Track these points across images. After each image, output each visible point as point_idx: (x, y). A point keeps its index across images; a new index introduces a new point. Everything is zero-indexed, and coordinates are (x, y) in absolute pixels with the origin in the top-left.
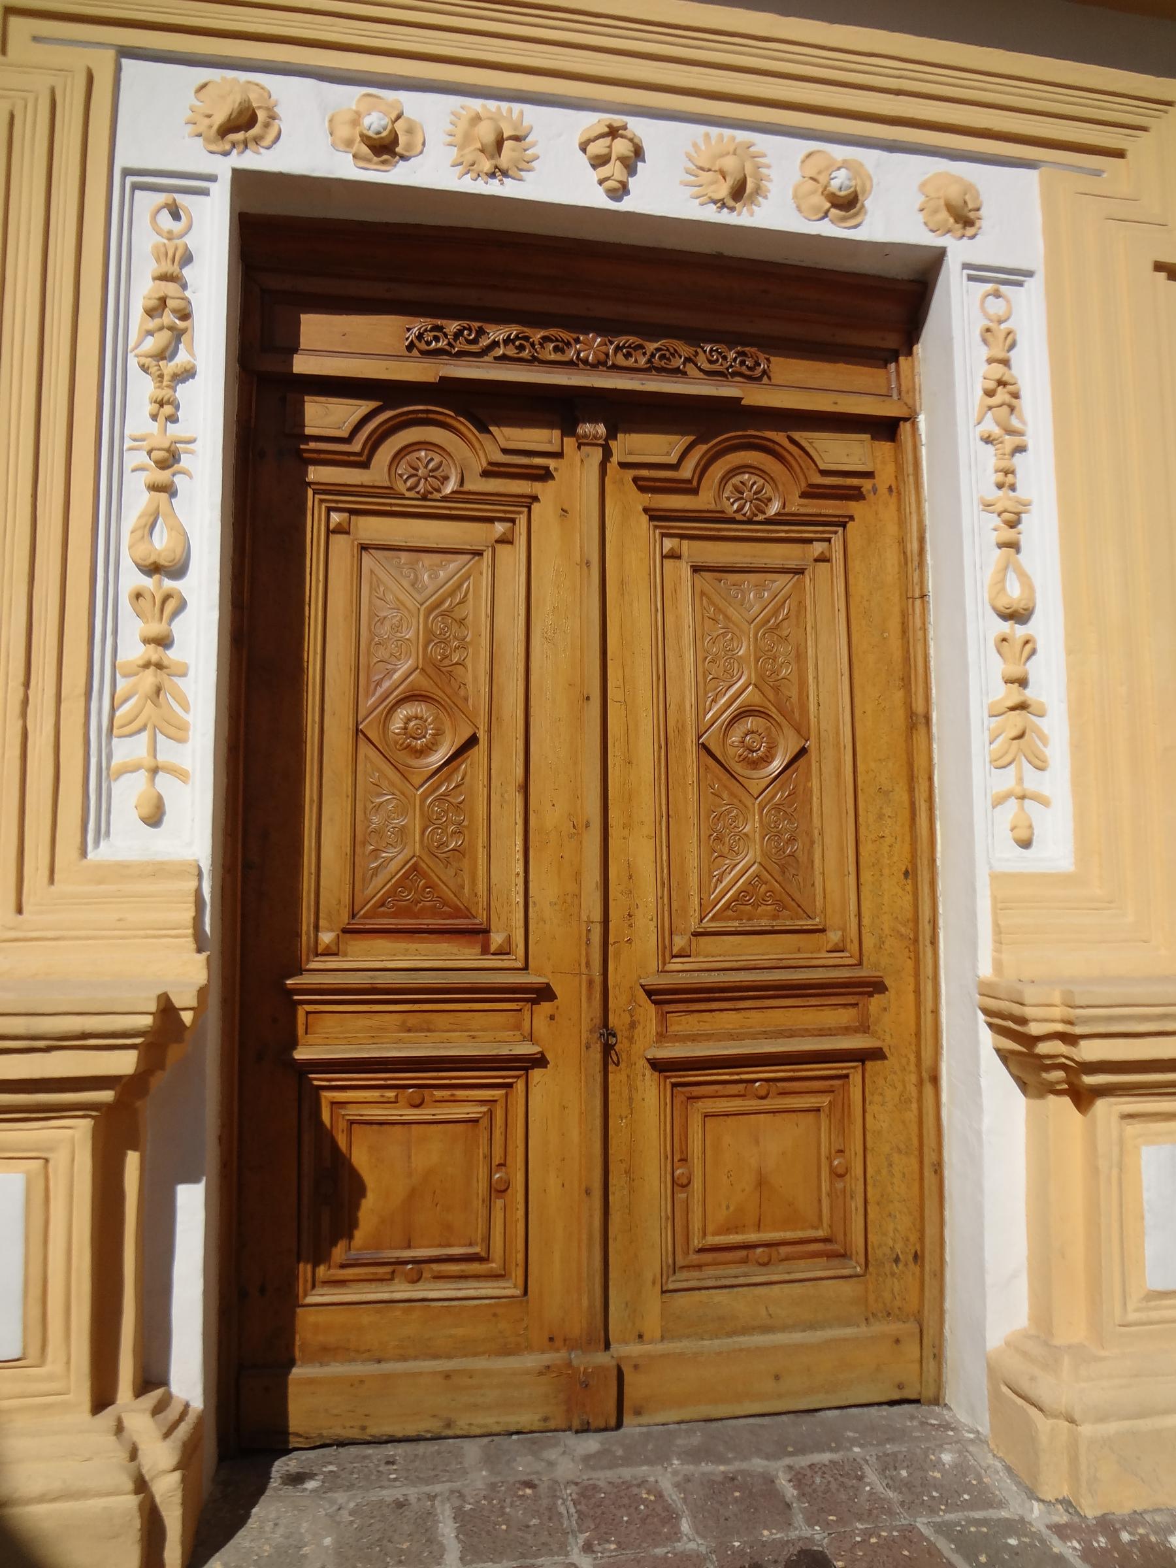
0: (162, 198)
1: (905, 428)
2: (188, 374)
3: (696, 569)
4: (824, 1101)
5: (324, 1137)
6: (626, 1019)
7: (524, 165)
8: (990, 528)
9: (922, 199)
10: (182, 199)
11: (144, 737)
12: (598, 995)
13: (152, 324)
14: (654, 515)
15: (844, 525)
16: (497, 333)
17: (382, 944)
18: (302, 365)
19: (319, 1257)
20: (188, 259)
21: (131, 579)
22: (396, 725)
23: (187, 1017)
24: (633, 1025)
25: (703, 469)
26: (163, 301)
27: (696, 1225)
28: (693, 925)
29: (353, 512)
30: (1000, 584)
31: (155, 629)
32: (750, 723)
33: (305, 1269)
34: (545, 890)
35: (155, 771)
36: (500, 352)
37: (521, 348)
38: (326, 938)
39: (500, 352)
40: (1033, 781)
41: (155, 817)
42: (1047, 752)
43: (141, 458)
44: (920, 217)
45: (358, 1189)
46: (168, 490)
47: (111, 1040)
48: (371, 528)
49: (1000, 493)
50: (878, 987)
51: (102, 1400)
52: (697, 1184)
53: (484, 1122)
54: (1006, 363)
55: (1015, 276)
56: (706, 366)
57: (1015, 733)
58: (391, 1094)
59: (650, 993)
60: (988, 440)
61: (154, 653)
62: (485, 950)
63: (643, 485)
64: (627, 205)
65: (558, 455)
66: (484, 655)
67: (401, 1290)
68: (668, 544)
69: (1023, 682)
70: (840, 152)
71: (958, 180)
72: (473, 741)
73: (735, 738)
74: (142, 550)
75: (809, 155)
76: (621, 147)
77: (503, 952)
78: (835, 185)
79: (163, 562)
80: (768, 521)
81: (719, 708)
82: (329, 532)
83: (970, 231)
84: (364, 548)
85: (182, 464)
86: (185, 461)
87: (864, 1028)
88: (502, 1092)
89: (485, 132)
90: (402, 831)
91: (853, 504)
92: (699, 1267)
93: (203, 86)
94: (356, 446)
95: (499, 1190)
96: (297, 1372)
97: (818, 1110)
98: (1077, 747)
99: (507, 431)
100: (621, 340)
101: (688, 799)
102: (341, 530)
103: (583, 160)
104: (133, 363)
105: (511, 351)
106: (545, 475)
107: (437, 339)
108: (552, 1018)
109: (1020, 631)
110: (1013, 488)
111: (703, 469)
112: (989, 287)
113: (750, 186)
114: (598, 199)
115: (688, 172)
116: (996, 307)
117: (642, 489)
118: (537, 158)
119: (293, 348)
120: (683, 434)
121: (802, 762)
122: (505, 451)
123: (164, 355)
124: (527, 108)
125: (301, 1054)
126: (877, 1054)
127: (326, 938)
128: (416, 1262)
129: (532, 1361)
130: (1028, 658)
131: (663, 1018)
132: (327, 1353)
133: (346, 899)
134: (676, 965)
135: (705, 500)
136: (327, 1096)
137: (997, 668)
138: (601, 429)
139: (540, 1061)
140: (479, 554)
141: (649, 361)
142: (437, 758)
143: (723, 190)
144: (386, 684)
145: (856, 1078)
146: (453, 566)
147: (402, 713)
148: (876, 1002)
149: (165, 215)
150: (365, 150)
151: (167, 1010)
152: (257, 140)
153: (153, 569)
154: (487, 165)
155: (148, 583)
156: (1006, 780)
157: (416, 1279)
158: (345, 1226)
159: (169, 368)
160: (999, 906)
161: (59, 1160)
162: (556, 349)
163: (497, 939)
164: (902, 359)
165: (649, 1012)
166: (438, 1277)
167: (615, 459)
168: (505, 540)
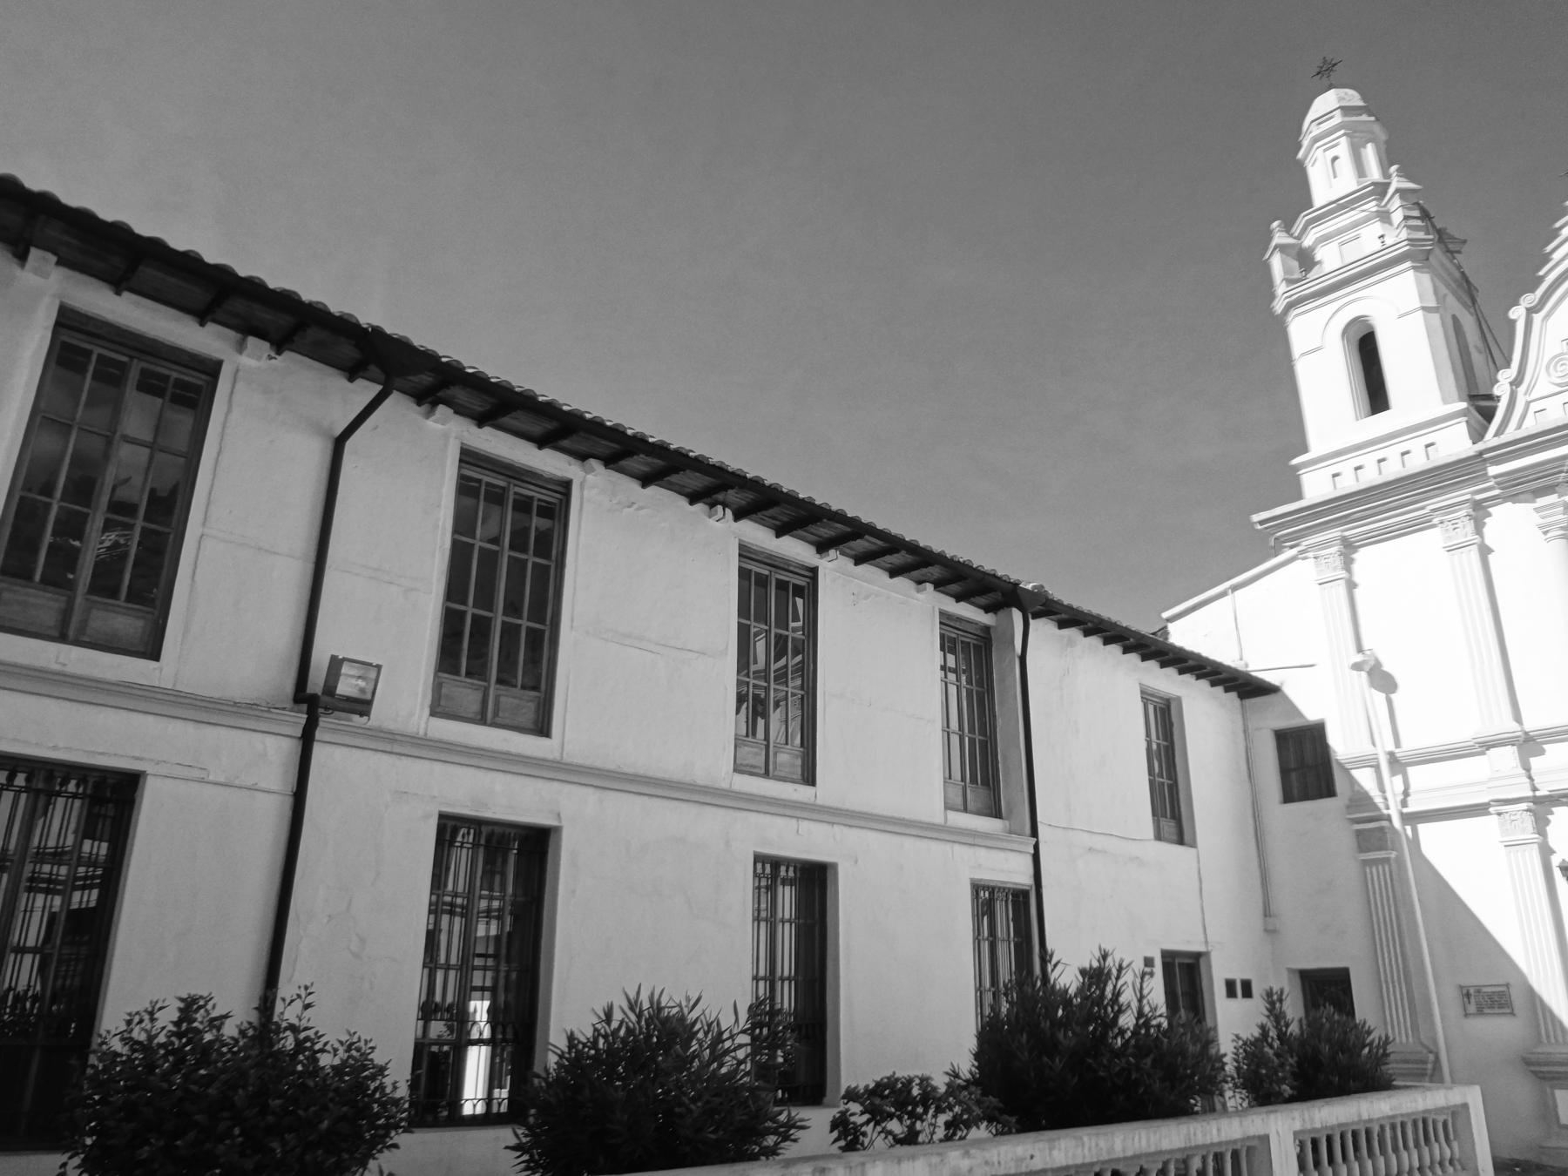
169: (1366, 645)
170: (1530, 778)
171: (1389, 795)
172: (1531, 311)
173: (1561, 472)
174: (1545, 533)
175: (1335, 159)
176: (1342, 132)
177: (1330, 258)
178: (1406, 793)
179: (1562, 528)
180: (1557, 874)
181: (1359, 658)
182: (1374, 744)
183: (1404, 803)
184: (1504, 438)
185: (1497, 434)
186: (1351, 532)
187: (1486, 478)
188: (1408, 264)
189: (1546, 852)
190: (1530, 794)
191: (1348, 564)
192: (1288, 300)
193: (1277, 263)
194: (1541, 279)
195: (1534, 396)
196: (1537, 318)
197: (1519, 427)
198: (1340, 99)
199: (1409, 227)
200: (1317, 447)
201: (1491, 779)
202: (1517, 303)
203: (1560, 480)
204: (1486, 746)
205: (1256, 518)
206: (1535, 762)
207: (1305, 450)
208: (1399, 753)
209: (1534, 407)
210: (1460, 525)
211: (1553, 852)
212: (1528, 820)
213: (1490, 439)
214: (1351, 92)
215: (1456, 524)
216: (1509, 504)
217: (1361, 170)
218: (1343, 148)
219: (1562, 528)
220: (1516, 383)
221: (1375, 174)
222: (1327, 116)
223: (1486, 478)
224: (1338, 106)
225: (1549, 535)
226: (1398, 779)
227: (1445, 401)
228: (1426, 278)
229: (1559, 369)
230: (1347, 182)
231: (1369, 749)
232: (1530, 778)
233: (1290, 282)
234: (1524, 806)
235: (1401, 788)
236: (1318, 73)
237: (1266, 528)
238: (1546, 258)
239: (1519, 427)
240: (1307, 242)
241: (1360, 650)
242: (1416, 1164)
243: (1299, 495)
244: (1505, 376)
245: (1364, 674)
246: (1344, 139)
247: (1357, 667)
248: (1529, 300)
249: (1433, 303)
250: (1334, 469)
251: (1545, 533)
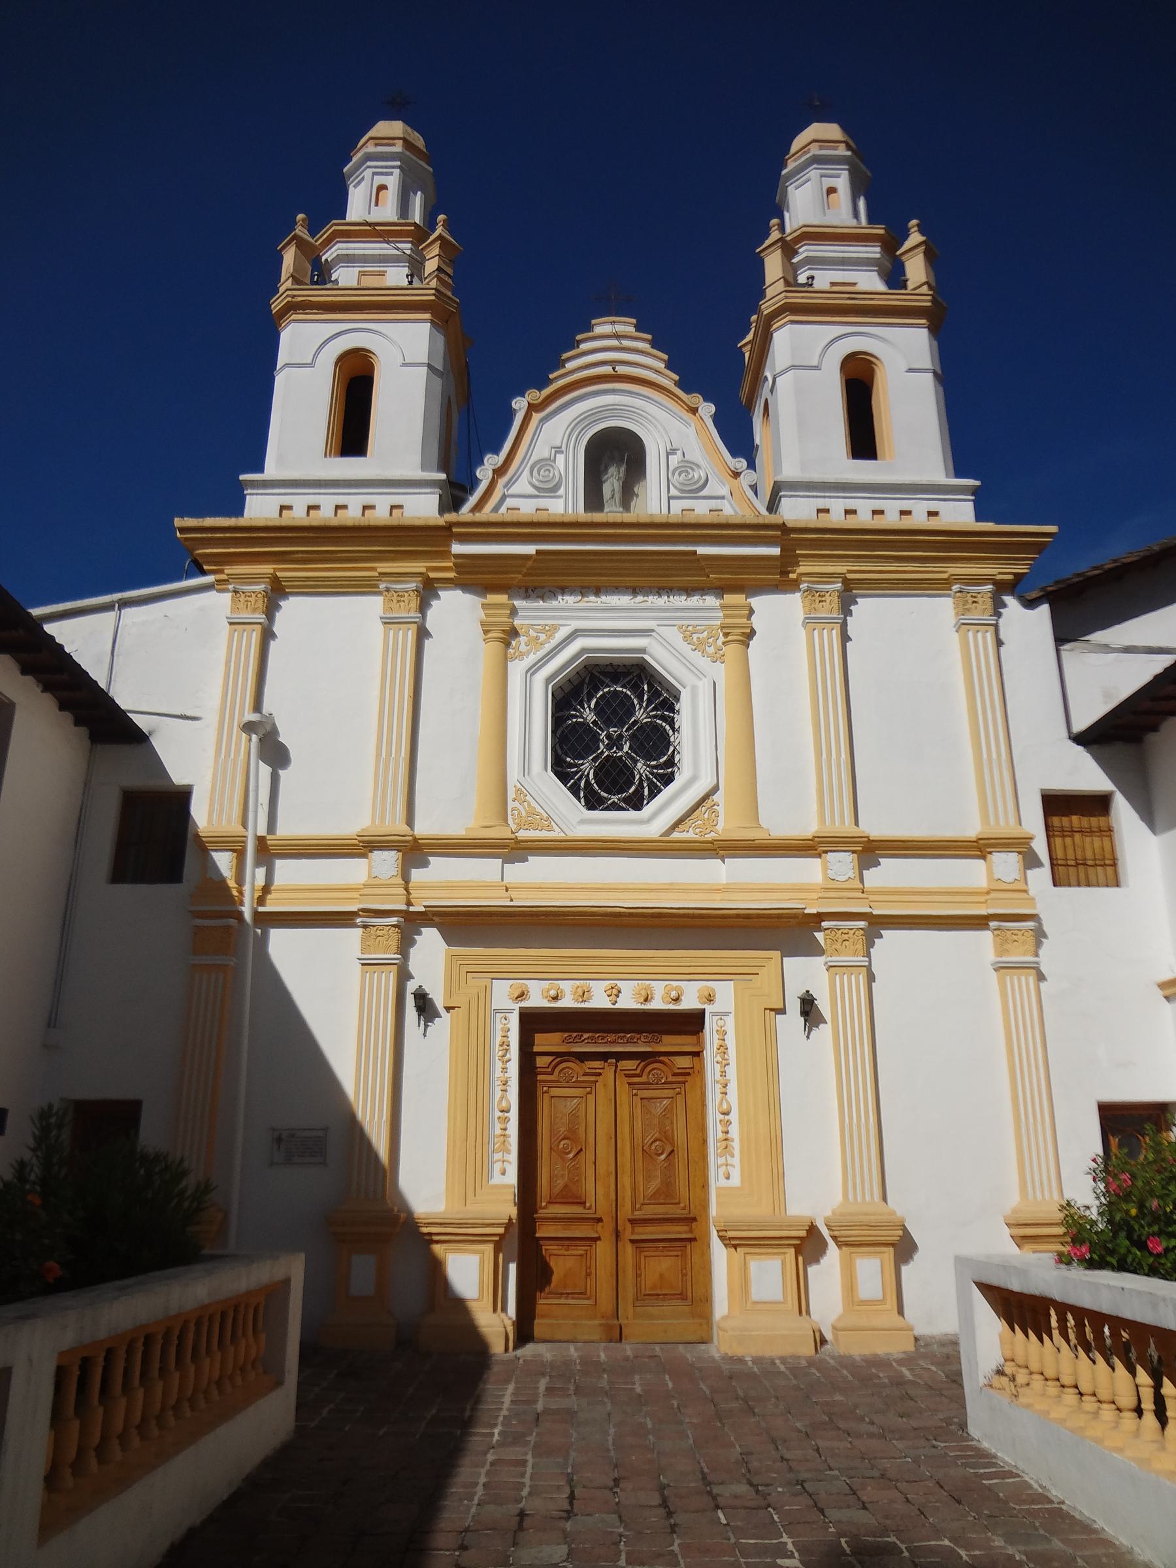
0: (502, 1015)
1: (701, 1054)
2: (509, 1060)
3: (641, 1099)
4: (679, 1253)
5: (543, 1258)
6: (623, 1228)
7: (590, 998)
8: (718, 1087)
9: (698, 994)
10: (507, 1014)
11: (501, 1153)
12: (614, 1220)
13: (501, 1048)
14: (630, 1084)
15: (685, 1084)
16: (586, 1035)
17: (558, 1206)
18: (536, 1049)
19: (542, 1290)
20: (509, 1030)
21: (498, 1114)
22: (561, 1146)
23: (514, 1221)
24: (625, 1229)
25: (643, 1070)
26: (504, 1042)
27: (643, 1287)
28: (642, 1200)
29: (549, 1087)
30: (721, 1104)
31: (503, 1126)
32: (658, 1143)
33: (538, 1294)
34: (600, 1191)
35: (503, 1162)
36: (586, 1041)
37: (592, 1040)
38: (543, 1204)
39: (586, 1041)
40: (730, 1160)
41: (503, 1173)
42: (735, 1153)
43: (499, 1083)
44: (698, 1000)
45: (552, 1272)
46: (505, 1091)
48: (555, 1091)
49: (722, 1078)
50: (694, 1219)
51: (495, 1310)
52: (643, 1275)
53: (585, 1256)
54: (724, 1040)
55: (727, 1014)
56: (643, 1040)
57: (724, 1147)
58: (560, 1247)
59: (629, 1220)
60: (718, 1063)
61: (502, 1132)
62: (585, 1207)
63: (627, 1076)
64: (616, 1006)
65: (604, 1068)
66: (584, 1124)
67: (563, 1301)
68: (634, 1091)
69: (727, 1132)
70: (675, 984)
71: (708, 987)
72: (581, 1150)
73: (653, 1147)
74: (500, 1107)
75: (666, 986)
76: (615, 992)
77: (590, 1208)
78: (672, 996)
79: (505, 1109)
80: (662, 1084)
81: (648, 1139)
82: (543, 1093)
83: (712, 1002)
84: (552, 1097)
85: (509, 1084)
86: (509, 1083)
87: (691, 1231)
88: (589, 1248)
89: (580, 992)
90: (563, 1175)
91: (687, 1077)
92: (644, 1300)
93: (512, 985)
94: (550, 1070)
95: (588, 1274)
96: (536, 1322)
97: (677, 1256)
98: (741, 1151)
99: (589, 1062)
100: (620, 1035)
101: (639, 1164)
102: (546, 1092)
103: (605, 994)
104: (497, 1058)
105: (590, 1041)
106: (600, 1074)
107: (570, 1039)
108: (602, 1227)
109: (727, 1117)
110: (725, 1076)
111: (643, 1070)
112: (719, 1017)
113: (649, 998)
114: (609, 1006)
115: (633, 994)
116: (721, 1023)
117: (626, 1077)
118: (593, 995)
119: (533, 1044)
120: (637, 1060)
121: (673, 1154)
122: (589, 1068)
123: (504, 1056)
124: (591, 981)
125: (537, 1235)
126: (694, 1239)
127: (543, 1204)
128: (567, 1293)
129: (597, 1322)
130: (729, 1125)
131: (633, 1228)
132: (543, 1317)
133: (549, 1193)
134: (636, 1213)
135: (644, 1079)
136: (543, 1247)
137: (720, 1128)
138: (614, 1061)
139: (599, 1239)
140: (583, 1097)
141: (627, 1040)
142: (571, 1156)
143: (642, 1000)
144: (558, 1135)
145: (689, 1247)
146: (576, 1101)
147: (562, 1143)
148: (694, 1225)
149: (503, 1019)
150: (551, 999)
151: (510, 1219)
152: (524, 999)
153: (502, 1111)
154: (581, 1000)
155: (501, 1114)
156: (721, 1160)
157: (567, 1298)
158: (549, 1282)
159: (506, 1058)
160: (718, 1196)
161: (486, 1254)
162: (602, 1039)
163: (588, 1205)
164: (700, 1034)
165: (629, 1226)
166: (573, 1298)
167: (619, 1068)
168: (589, 1093)
169: (267, 708)
170: (407, 889)
171: (247, 889)
172: (532, 408)
173: (519, 573)
174: (486, 632)
175: (382, 187)
176: (398, 163)
177: (345, 276)
178: (266, 889)
180: (410, 1002)
181: (254, 717)
182: (244, 825)
183: (261, 901)
184: (479, 517)
185: (474, 510)
186: (286, 573)
187: (446, 554)
188: (428, 316)
189: (404, 976)
190: (404, 907)
191: (271, 610)
192: (290, 299)
193: (289, 258)
194: (549, 382)
195: (512, 491)
196: (536, 417)
198: (405, 132)
199: (439, 279)
200: (272, 469)
201: (365, 886)
203: (515, 583)
204: (365, 846)
205: (178, 522)
206: (416, 874)
207: (260, 468)
208: (271, 840)
209: (509, 502)
210: (406, 599)
211: (410, 977)
212: (394, 937)
213: (465, 513)
215: (401, 596)
216: (459, 592)
217: (404, 207)
218: (393, 181)
220: (499, 472)
221: (417, 216)
222: (389, 140)
223: (446, 554)
224: (402, 136)
225: (490, 635)
226: (261, 872)
227: (424, 468)
228: (440, 339)
229: (542, 472)
230: (388, 211)
231: (235, 828)
232: (407, 889)
233: (296, 281)
234: (393, 920)
235: (260, 881)
237: (186, 539)
238: (560, 364)
240: (328, 256)
241: (257, 706)
242: (216, 1374)
243: (239, 511)
244: (491, 461)
245: (254, 737)
246: (397, 172)
247: (249, 727)
248: (534, 396)
249: (439, 366)
250: (286, 500)
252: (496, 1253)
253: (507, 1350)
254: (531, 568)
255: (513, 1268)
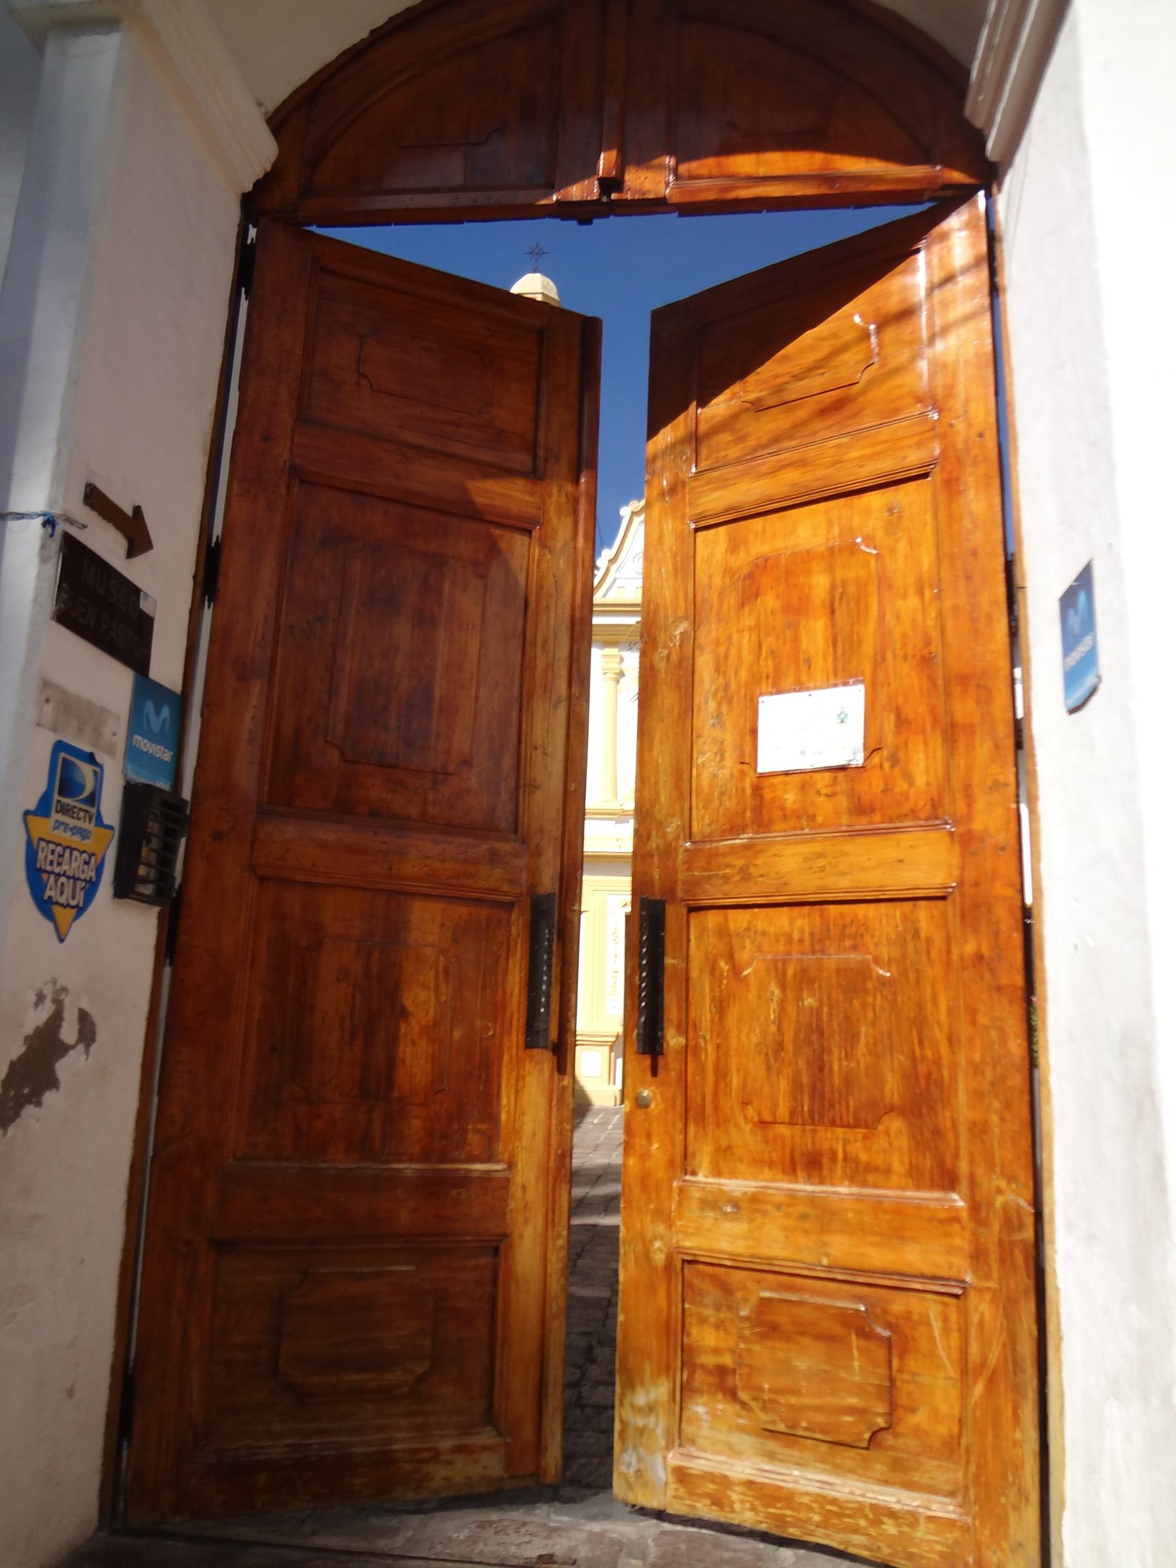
47: (612, 1036)
172: (634, 514)
179: (615, 673)
197: (604, 596)
198: (544, 286)
202: (627, 504)
209: (618, 583)
214: (551, 284)
219: (615, 673)
220: (612, 561)
224: (541, 291)
236: (531, 253)
239: (604, 596)
251: (605, 674)
252: (611, 1052)
253: (615, 1105)
254: (633, 631)
255: (620, 1061)
